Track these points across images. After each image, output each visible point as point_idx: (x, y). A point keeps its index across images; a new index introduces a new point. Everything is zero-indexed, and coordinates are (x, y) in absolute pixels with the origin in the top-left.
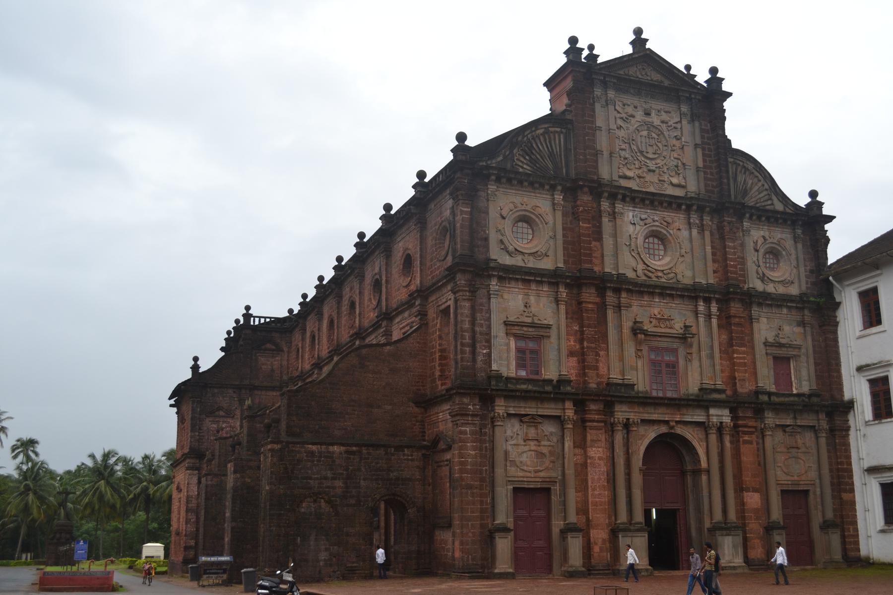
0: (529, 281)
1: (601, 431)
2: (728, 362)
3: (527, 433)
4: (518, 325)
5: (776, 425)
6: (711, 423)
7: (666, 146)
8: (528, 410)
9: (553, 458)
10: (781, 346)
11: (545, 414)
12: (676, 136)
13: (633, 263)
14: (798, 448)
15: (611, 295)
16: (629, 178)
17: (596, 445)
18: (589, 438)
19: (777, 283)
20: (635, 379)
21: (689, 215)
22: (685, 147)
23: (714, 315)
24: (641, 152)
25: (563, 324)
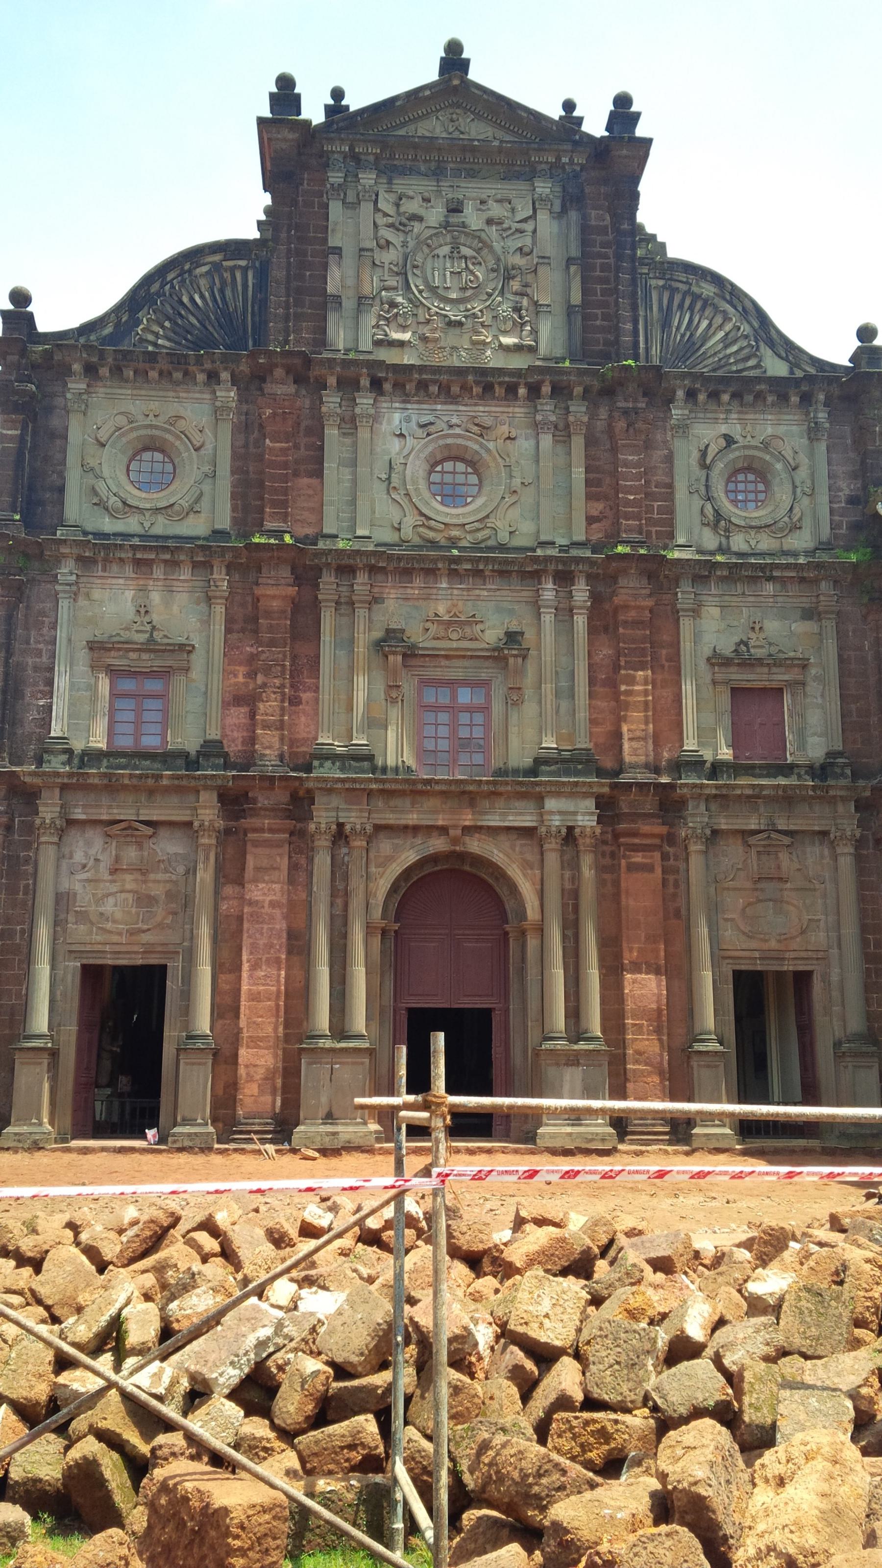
0: (149, 563)
1: (280, 851)
2: (613, 704)
3: (117, 859)
4: (119, 649)
5: (715, 832)
6: (543, 830)
7: (493, 270)
8: (115, 811)
9: (174, 905)
10: (749, 663)
11: (155, 818)
12: (521, 249)
13: (395, 515)
14: (780, 879)
15: (333, 579)
16: (401, 344)
17: (266, 878)
18: (251, 862)
19: (753, 533)
20: (383, 745)
21: (536, 407)
22: (541, 270)
23: (581, 608)
24: (433, 290)
25: (217, 641)
